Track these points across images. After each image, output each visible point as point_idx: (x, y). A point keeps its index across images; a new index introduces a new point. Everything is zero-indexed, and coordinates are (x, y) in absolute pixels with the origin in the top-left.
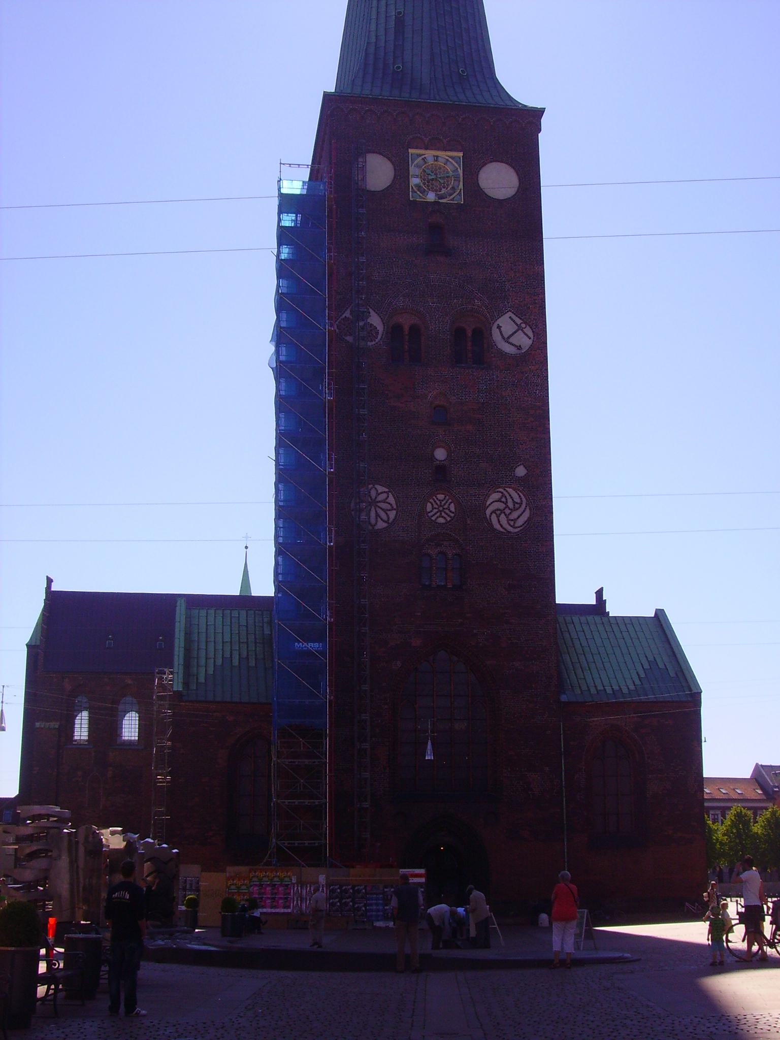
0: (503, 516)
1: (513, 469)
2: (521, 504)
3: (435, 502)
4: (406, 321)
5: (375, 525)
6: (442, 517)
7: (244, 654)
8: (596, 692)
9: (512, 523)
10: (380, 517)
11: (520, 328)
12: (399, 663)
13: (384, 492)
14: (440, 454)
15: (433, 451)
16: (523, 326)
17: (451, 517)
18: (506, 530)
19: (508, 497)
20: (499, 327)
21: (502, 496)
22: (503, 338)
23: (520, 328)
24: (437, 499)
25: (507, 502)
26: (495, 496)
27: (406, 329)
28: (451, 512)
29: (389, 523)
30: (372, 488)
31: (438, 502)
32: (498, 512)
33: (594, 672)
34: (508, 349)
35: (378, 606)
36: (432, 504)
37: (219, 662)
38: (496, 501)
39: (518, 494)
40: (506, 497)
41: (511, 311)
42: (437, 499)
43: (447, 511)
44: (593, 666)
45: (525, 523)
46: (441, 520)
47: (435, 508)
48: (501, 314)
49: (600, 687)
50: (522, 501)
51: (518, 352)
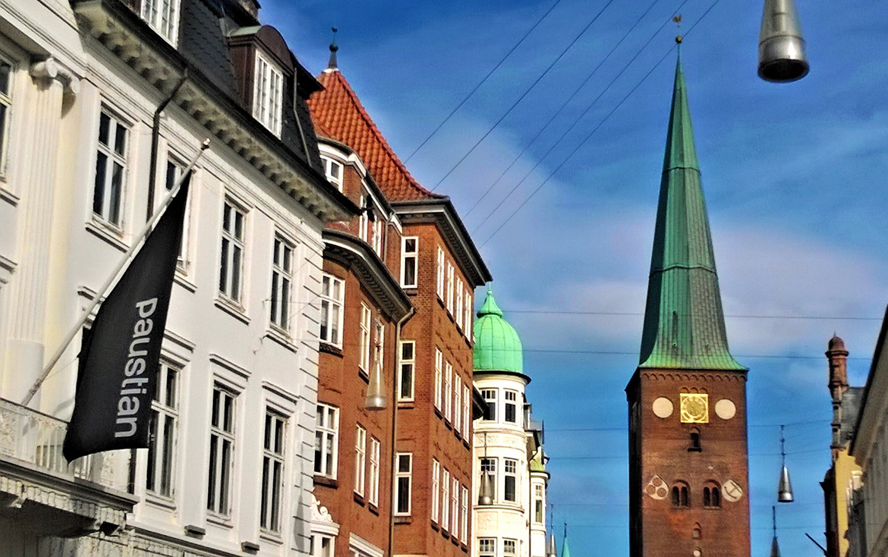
4: (680, 486)
22: (727, 493)
27: (680, 490)
34: (728, 498)
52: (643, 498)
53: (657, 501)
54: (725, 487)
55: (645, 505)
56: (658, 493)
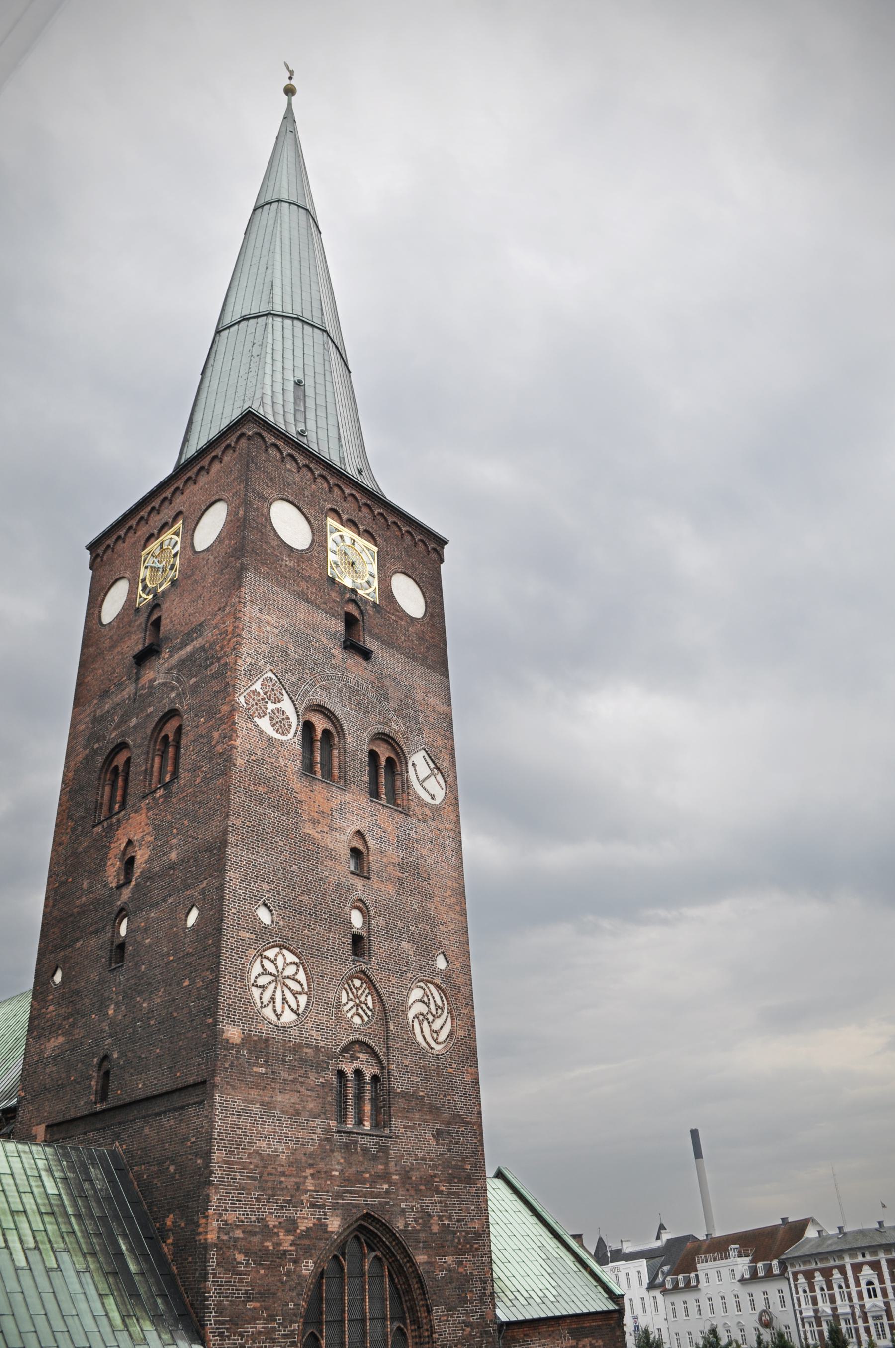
0: (425, 1022)
6: (359, 1015)
11: (432, 774)
19: (430, 997)
23: (432, 774)
24: (354, 985)
41: (425, 749)
45: (448, 1036)
54: (413, 764)
56: (272, 719)
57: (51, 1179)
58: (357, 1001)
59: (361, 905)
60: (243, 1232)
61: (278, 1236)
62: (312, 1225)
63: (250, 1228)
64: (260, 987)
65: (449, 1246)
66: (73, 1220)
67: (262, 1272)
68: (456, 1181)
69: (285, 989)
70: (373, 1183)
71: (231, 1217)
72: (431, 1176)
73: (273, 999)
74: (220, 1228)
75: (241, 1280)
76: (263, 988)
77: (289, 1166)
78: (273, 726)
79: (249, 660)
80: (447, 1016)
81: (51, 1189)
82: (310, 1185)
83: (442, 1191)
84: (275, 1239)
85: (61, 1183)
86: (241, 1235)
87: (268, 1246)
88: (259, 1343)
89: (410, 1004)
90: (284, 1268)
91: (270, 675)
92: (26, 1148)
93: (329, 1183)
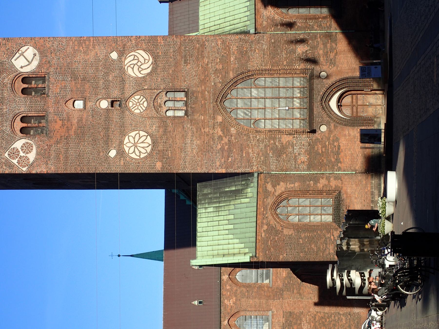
1: (113, 60)
2: (135, 56)
3: (134, 108)
4: (18, 125)
5: (149, 144)
6: (143, 103)
7: (226, 222)
8: (249, 12)
9: (146, 61)
10: (144, 141)
11: (22, 54)
12: (232, 129)
13: (128, 138)
14: (104, 104)
15: (102, 109)
16: (20, 52)
17: (143, 98)
18: (151, 65)
19: (131, 63)
20: (22, 67)
21: (130, 67)
23: (22, 54)
24: (132, 106)
25: (133, 64)
26: (130, 71)
28: (140, 98)
29: (148, 136)
30: (126, 146)
31: (134, 105)
32: (140, 69)
33: (236, 12)
35: (198, 142)
36: (136, 109)
37: (231, 236)
38: (133, 71)
39: (128, 57)
40: (130, 65)
41: (11, 60)
42: (132, 106)
43: (140, 100)
44: (232, 13)
46: (145, 104)
47: (138, 107)
48: (13, 66)
49: (246, 9)
50: (133, 55)
51: (37, 55)
52: (34, 172)
53: (37, 154)
54: (22, 67)
55: (42, 169)
56: (27, 153)
57: (208, 208)
58: (138, 104)
59: (98, 102)
60: (222, 158)
61: (224, 143)
62: (220, 129)
63: (221, 156)
64: (140, 154)
65: (227, 60)
66: (220, 205)
67: (234, 150)
68: (203, 53)
69: (139, 142)
70: (205, 99)
71: (218, 164)
72: (202, 67)
73: (143, 148)
74: (221, 168)
75: (237, 159)
76: (140, 152)
77: (201, 139)
78: (30, 152)
79: (4, 167)
80: (136, 52)
81: (211, 210)
82: (207, 130)
83: (207, 61)
84: (224, 145)
85: (209, 205)
86: (223, 159)
87: (227, 148)
88: (255, 151)
89: (135, 76)
90: (233, 141)
91: (6, 155)
92: (199, 214)
93: (206, 121)
